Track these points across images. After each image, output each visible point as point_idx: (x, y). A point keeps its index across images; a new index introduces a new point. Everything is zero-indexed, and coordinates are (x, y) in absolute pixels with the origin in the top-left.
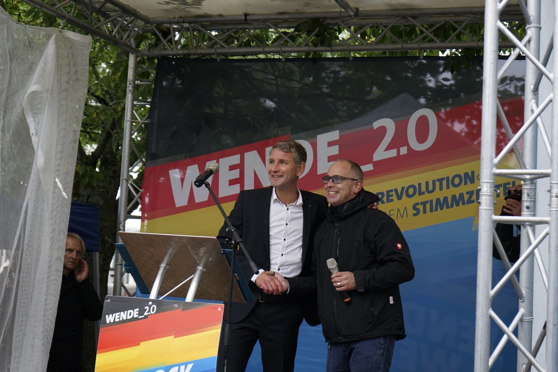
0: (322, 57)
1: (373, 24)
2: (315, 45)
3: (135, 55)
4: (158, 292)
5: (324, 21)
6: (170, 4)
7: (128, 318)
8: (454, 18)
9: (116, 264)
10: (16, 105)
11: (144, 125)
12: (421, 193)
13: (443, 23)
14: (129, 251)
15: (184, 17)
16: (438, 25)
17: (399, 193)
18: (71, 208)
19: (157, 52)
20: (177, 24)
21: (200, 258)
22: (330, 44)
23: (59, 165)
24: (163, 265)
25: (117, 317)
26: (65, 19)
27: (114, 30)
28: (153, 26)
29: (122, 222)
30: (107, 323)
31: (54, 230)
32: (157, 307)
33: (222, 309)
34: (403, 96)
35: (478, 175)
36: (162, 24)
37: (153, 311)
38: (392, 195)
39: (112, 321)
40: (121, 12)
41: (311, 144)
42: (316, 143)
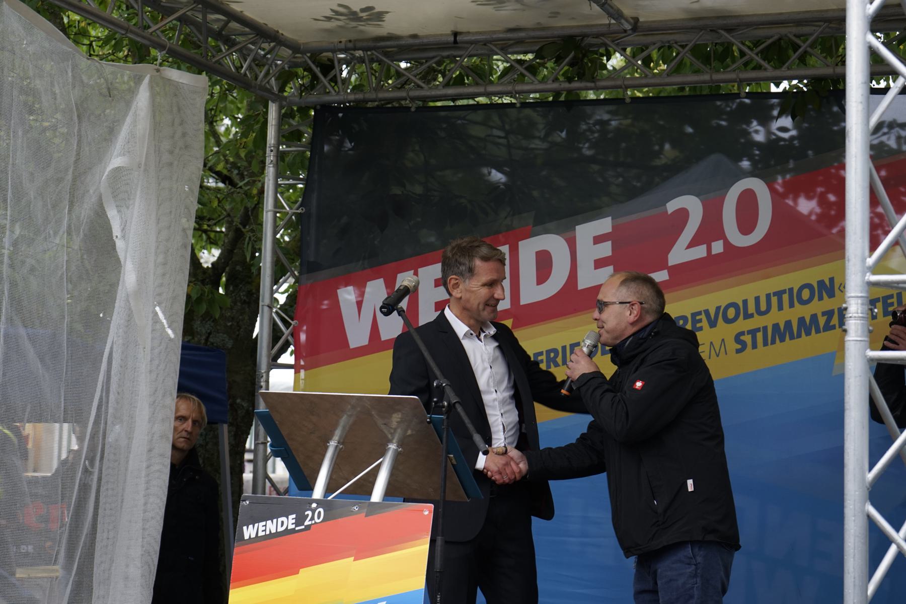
0: (581, 99)
1: (662, 42)
2: (570, 80)
3: (277, 103)
4: (325, 488)
5: (582, 40)
6: (333, 20)
7: (278, 531)
8: (795, 30)
9: (257, 442)
10: (88, 191)
11: (295, 217)
12: (748, 316)
13: (776, 37)
14: (277, 422)
15: (355, 41)
16: (769, 41)
17: (713, 317)
18: (182, 354)
19: (314, 97)
20: (344, 52)
21: (392, 431)
22: (593, 78)
23: (161, 285)
24: (333, 443)
25: (261, 528)
26: (165, 50)
27: (243, 64)
28: (305, 57)
29: (264, 375)
30: (245, 539)
31: (156, 391)
32: (324, 511)
33: (430, 512)
34: (714, 157)
35: (839, 285)
36: (322, 53)
37: (319, 518)
39: (253, 536)
40: (255, 35)
41: (568, 241)
42: (574, 238)
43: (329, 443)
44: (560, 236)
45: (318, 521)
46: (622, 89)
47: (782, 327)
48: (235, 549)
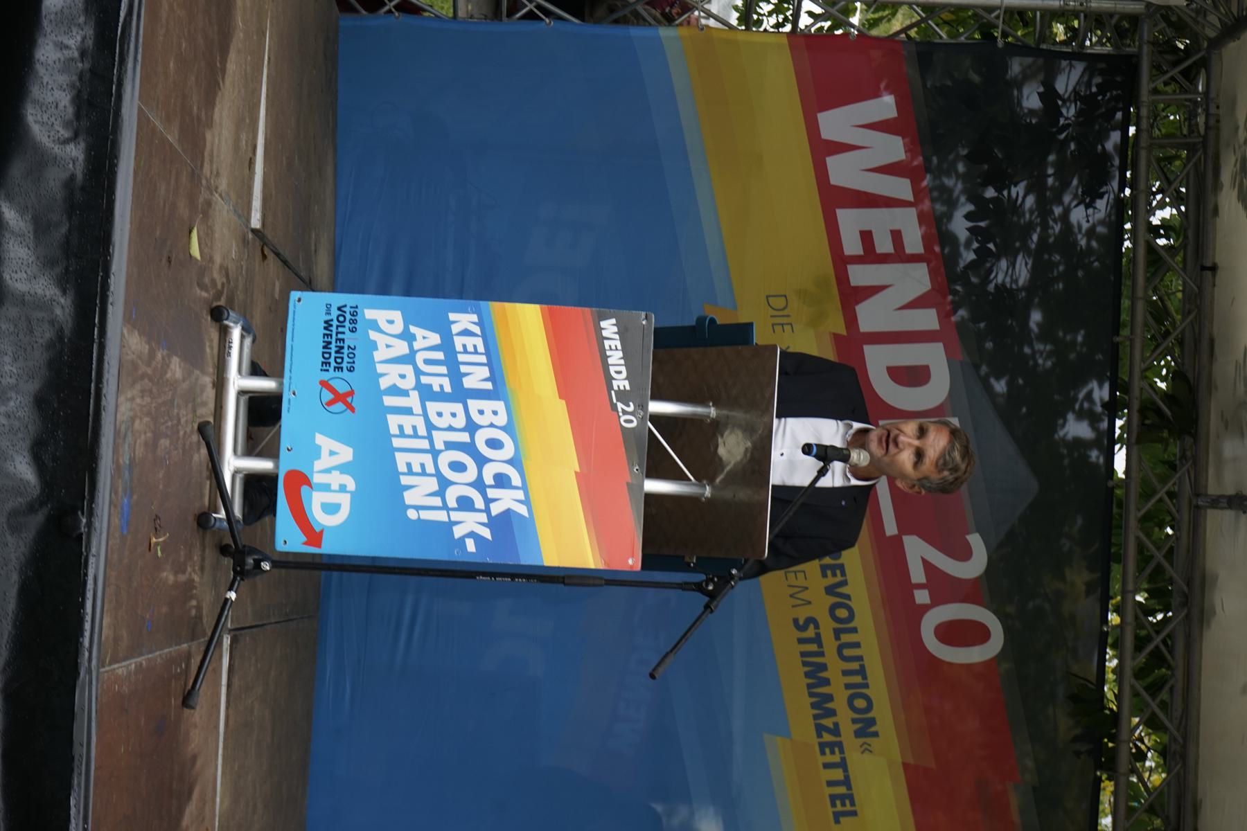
0: (1111, 563)
8: (1179, 686)
12: (837, 633)
13: (1172, 663)
14: (740, 348)
15: (1218, 129)
25: (613, 343)
32: (633, 429)
33: (632, 567)
37: (626, 421)
38: (834, 575)
39: (605, 333)
40: (1236, 15)
43: (713, 406)
44: (946, 398)
45: (623, 418)
46: (1129, 333)
47: (823, 674)
48: (586, 309)
